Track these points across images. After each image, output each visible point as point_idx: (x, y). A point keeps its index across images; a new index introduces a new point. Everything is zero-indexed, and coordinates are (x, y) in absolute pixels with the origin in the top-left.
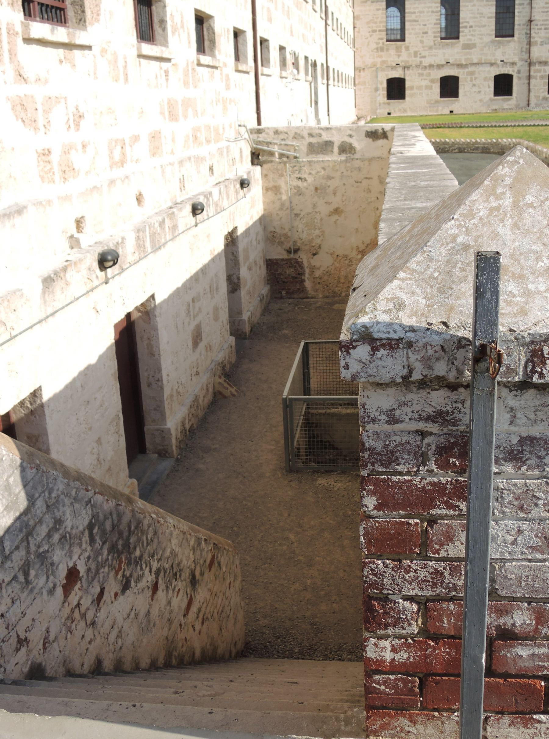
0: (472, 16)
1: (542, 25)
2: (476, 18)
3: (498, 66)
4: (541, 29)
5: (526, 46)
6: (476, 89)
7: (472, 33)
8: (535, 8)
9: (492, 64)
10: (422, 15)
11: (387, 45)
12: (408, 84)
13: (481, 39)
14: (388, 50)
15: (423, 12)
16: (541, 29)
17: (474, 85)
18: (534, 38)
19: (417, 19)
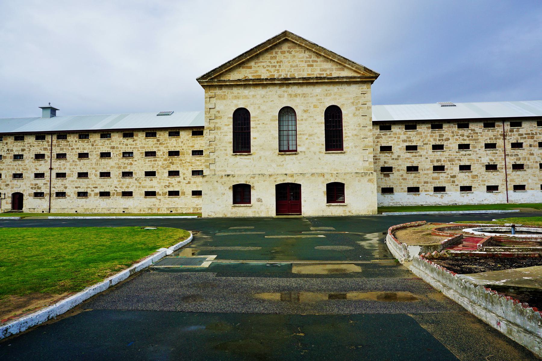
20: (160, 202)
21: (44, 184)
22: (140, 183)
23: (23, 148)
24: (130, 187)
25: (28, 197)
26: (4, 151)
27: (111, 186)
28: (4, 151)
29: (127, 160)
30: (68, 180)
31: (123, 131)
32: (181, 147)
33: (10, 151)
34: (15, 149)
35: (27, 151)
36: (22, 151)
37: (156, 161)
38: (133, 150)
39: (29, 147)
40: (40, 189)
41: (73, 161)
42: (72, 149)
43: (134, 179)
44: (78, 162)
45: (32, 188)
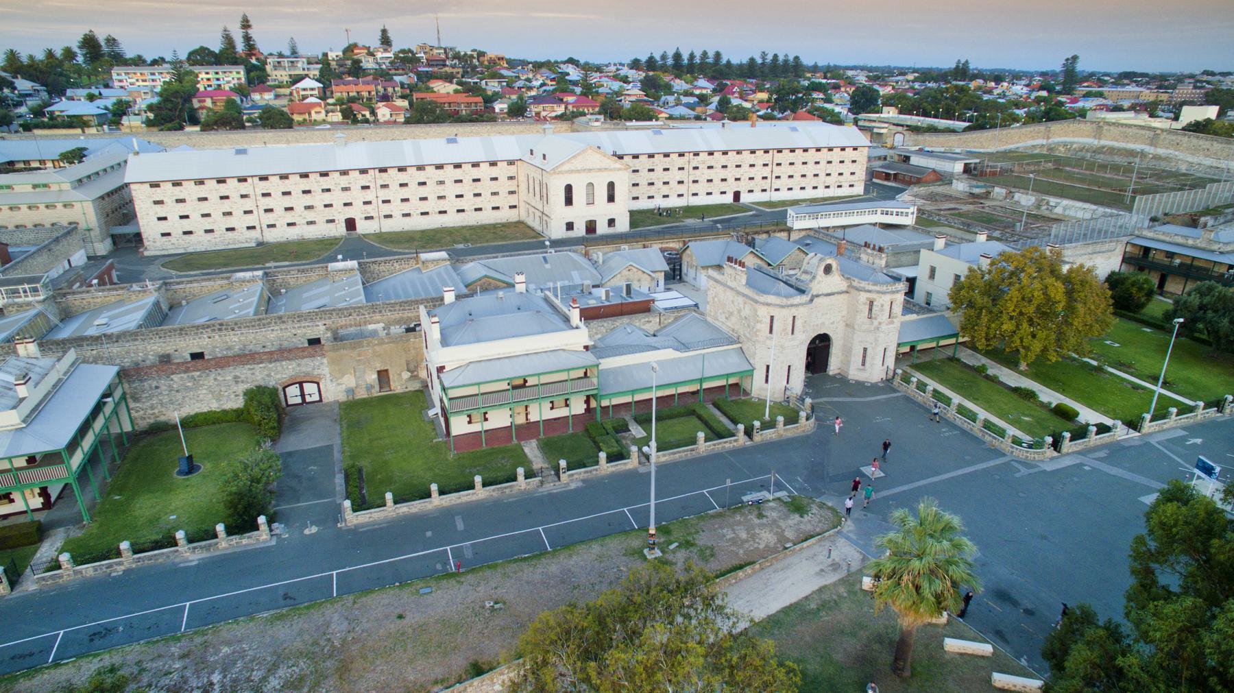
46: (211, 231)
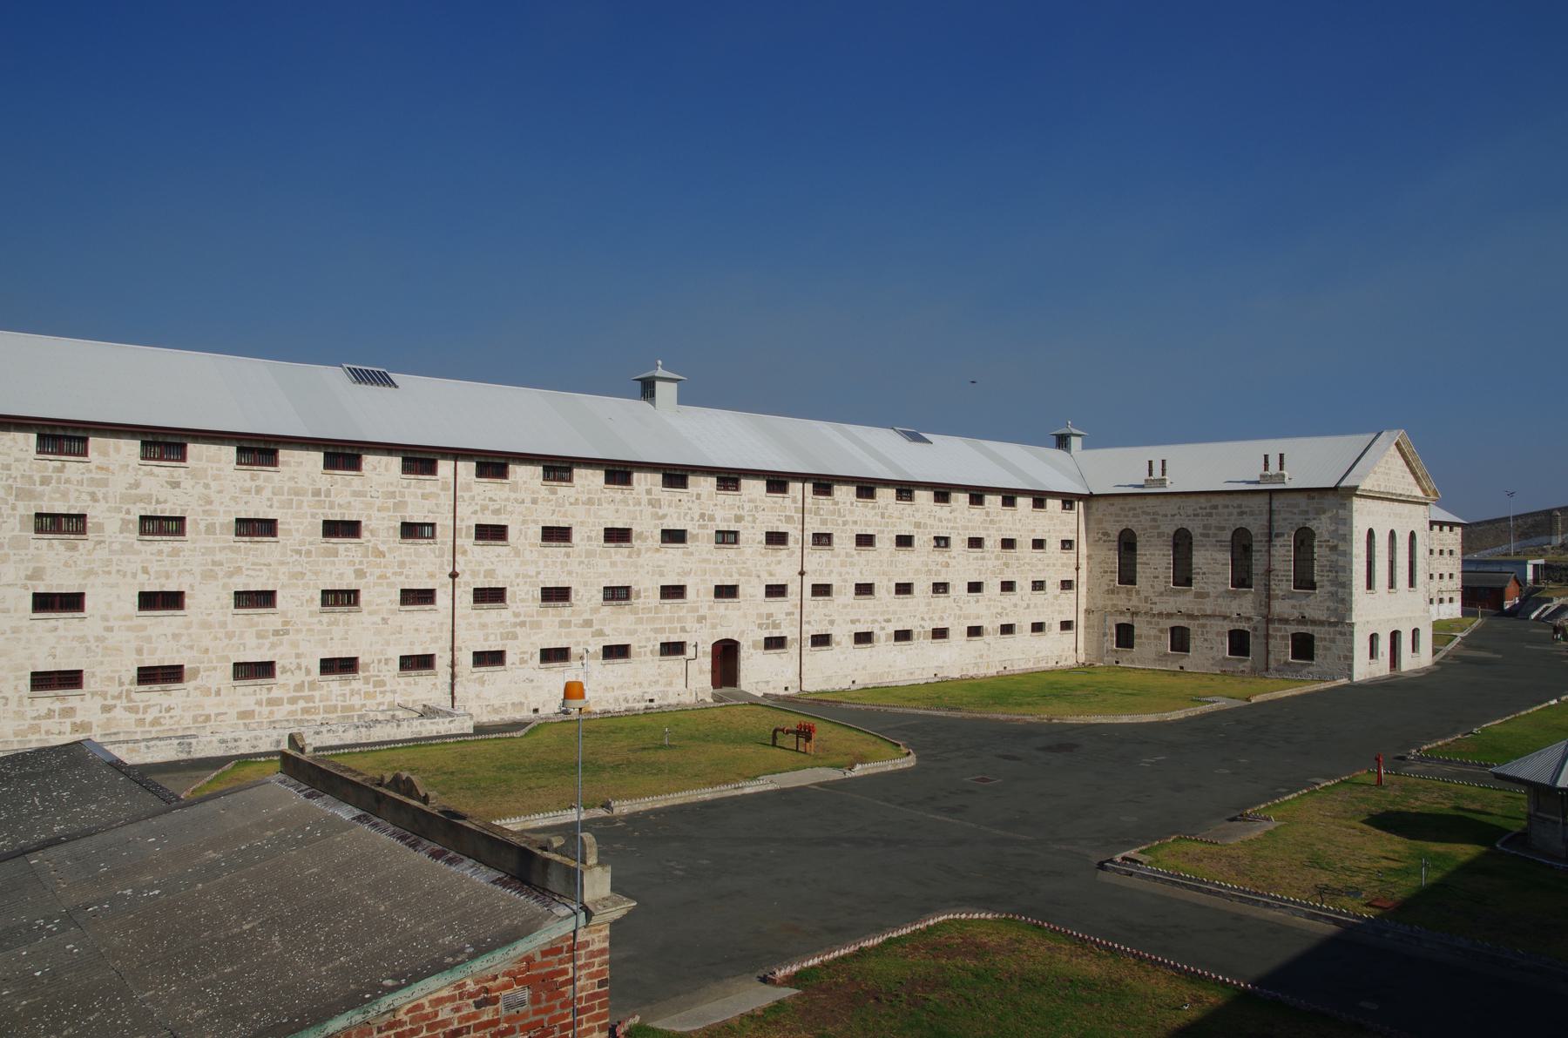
0: (1204, 561)
1: (1284, 576)
2: (1210, 564)
3: (1232, 621)
4: (1282, 580)
5: (1264, 600)
6: (1206, 644)
7: (1205, 580)
8: (1274, 556)
9: (1225, 617)
10: (1153, 557)
11: (1117, 587)
12: (1136, 632)
13: (1215, 588)
14: (1118, 593)
15: (1154, 555)
16: (1282, 580)
17: (1206, 640)
18: (1274, 590)
19: (1147, 562)
20: (989, 650)
21: (788, 614)
22: (961, 608)
23: (739, 513)
24: (945, 617)
25: (752, 651)
26: (692, 519)
27: (915, 616)
28: (692, 519)
29: (941, 557)
30: (836, 602)
31: (935, 487)
32: (1019, 531)
33: (706, 518)
34: (719, 514)
35: (748, 522)
36: (736, 522)
37: (983, 558)
38: (950, 534)
39: (752, 511)
40: (777, 628)
41: (847, 555)
42: (845, 523)
43: (951, 599)
44: (856, 557)
45: (760, 626)
46: (264, 670)
